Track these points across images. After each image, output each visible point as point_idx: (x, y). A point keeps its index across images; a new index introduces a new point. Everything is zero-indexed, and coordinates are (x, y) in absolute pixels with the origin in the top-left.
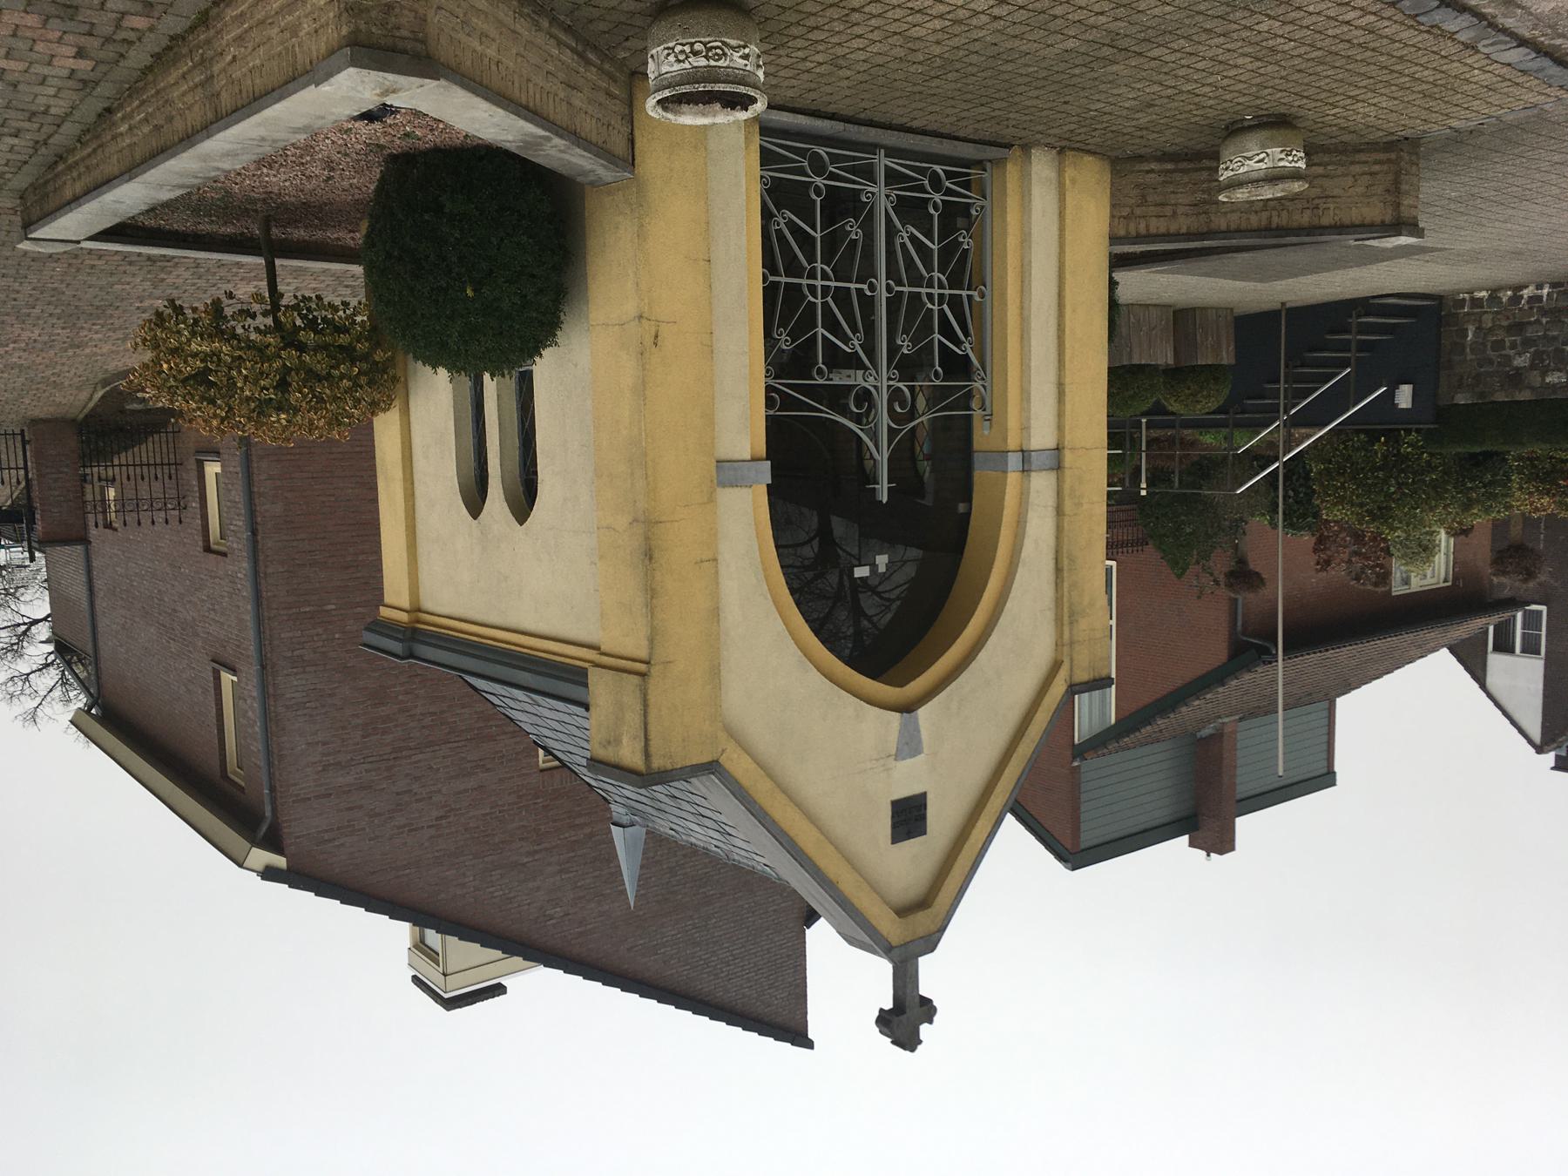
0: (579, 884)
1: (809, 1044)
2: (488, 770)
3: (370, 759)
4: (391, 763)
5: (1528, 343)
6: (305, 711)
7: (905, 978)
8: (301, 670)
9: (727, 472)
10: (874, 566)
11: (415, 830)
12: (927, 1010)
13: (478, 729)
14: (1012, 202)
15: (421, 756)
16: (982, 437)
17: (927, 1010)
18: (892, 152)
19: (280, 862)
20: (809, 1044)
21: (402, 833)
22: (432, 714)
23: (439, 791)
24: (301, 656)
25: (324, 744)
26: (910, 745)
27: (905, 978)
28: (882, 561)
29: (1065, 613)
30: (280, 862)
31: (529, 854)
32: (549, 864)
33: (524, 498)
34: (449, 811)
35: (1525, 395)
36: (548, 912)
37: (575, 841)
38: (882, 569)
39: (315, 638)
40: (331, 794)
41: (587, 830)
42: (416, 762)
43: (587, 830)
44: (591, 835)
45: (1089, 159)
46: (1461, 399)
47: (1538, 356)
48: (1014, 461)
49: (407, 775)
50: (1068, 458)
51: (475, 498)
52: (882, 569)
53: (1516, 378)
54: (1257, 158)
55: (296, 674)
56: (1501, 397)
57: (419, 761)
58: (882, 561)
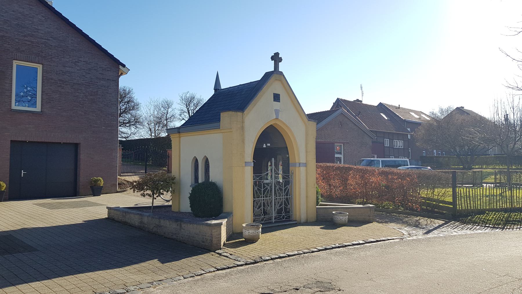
0: (31, 22)
2: (61, 71)
3: (96, 85)
4: (91, 83)
6: (112, 103)
7: (276, 66)
8: (112, 113)
10: (266, 145)
11: (86, 62)
12: (273, 58)
13: (64, 84)
15: (83, 82)
17: (273, 58)
18: (271, 223)
21: (89, 62)
22: (78, 92)
23: (78, 70)
24: (112, 117)
25: (108, 93)
27: (276, 66)
28: (264, 146)
30: (121, 67)
31: (49, 40)
32: (42, 34)
34: (74, 63)
36: (44, 19)
37: (32, 37)
38: (265, 144)
39: (108, 120)
40: (107, 79)
41: (26, 38)
42: (84, 80)
43: (26, 38)
44: (25, 36)
45: (239, 232)
49: (87, 78)
50: (244, 165)
52: (265, 144)
54: (250, 233)
55: (113, 113)
57: (83, 80)
58: (264, 146)
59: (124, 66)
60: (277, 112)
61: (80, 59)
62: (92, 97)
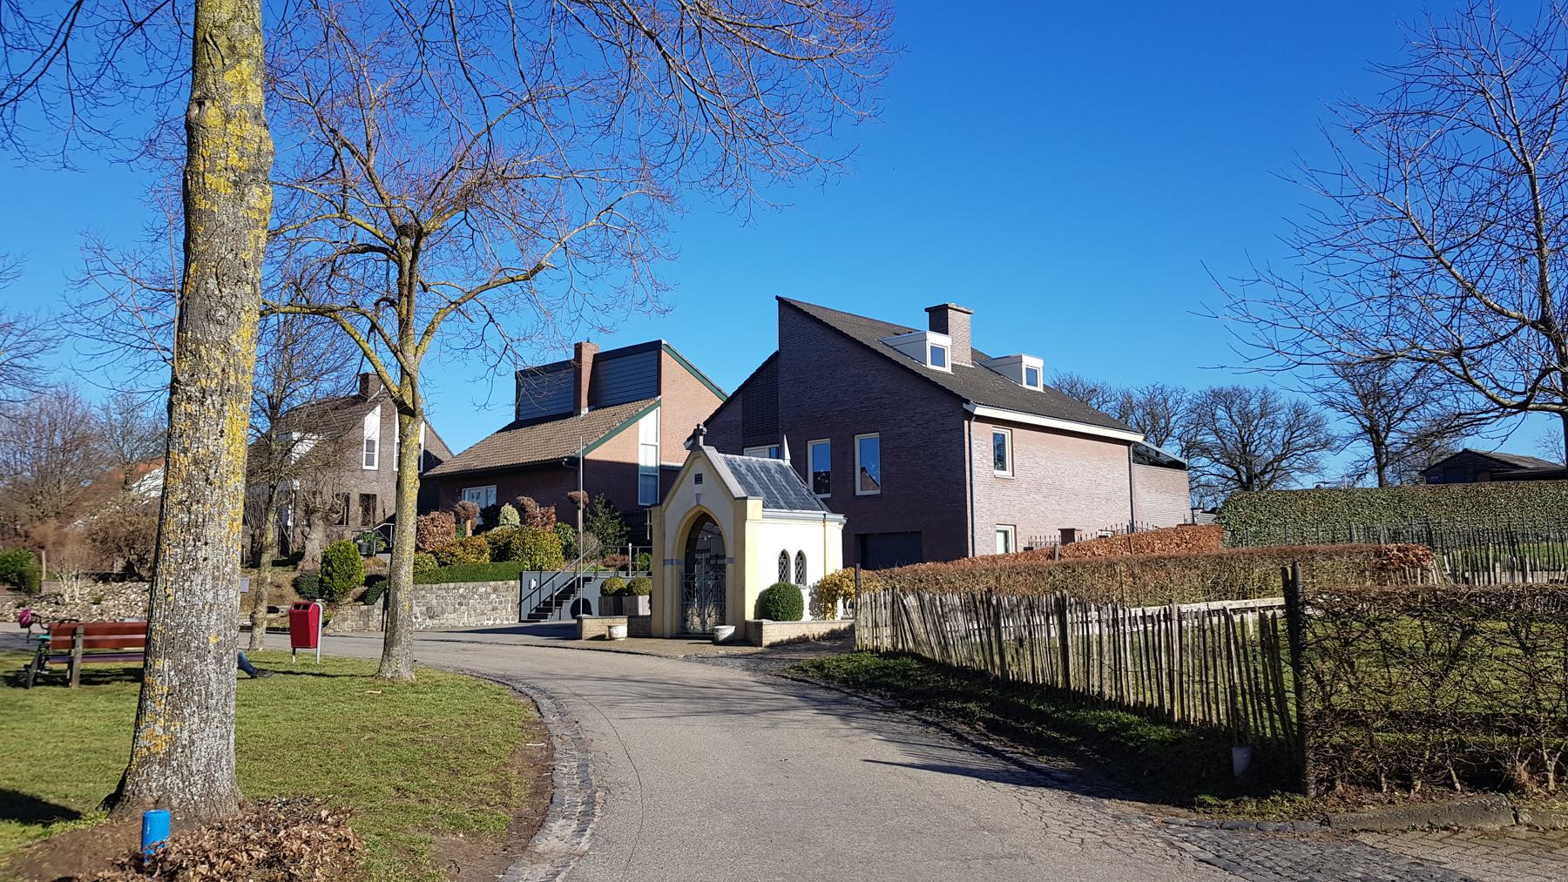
1: (777, 298)
5: (491, 603)
9: (732, 560)
14: (675, 625)
16: (682, 567)
19: (965, 406)
20: (777, 298)
26: (698, 496)
29: (662, 524)
30: (965, 406)
33: (784, 555)
35: (492, 583)
46: (512, 583)
47: (488, 598)
48: (675, 562)
51: (800, 555)
53: (495, 590)
56: (500, 583)
59: (967, 402)
60: (698, 496)
61: (917, 411)
62: (932, 462)
